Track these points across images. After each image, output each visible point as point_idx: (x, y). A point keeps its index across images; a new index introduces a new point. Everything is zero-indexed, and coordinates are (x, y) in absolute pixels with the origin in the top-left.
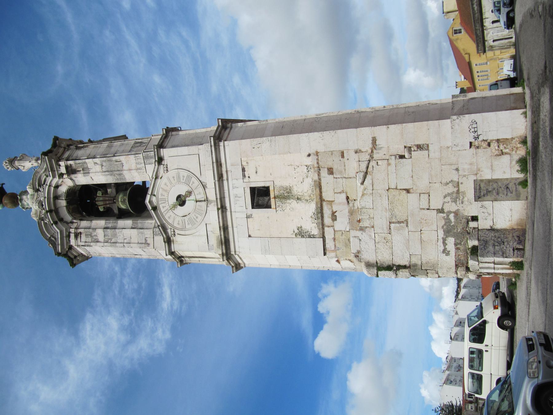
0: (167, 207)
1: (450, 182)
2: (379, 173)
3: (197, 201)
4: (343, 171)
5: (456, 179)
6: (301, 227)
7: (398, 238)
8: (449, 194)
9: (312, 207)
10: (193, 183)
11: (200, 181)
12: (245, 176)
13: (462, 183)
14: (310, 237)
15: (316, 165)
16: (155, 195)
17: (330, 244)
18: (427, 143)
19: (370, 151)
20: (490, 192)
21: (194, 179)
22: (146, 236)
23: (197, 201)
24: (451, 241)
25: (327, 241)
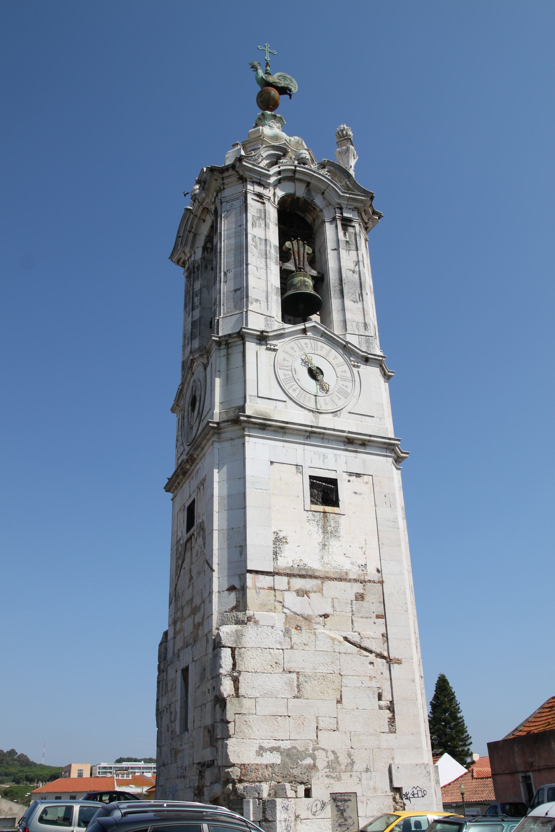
0: (307, 351)
1: (352, 760)
2: (357, 664)
4: (362, 615)
5: (356, 767)
6: (287, 543)
7: (277, 682)
8: (337, 758)
9: (314, 563)
10: (339, 399)
12: (350, 475)
13: (351, 776)
14: (275, 553)
15: (367, 578)
18: (397, 732)
20: (342, 814)
24: (275, 759)
25: (269, 578)
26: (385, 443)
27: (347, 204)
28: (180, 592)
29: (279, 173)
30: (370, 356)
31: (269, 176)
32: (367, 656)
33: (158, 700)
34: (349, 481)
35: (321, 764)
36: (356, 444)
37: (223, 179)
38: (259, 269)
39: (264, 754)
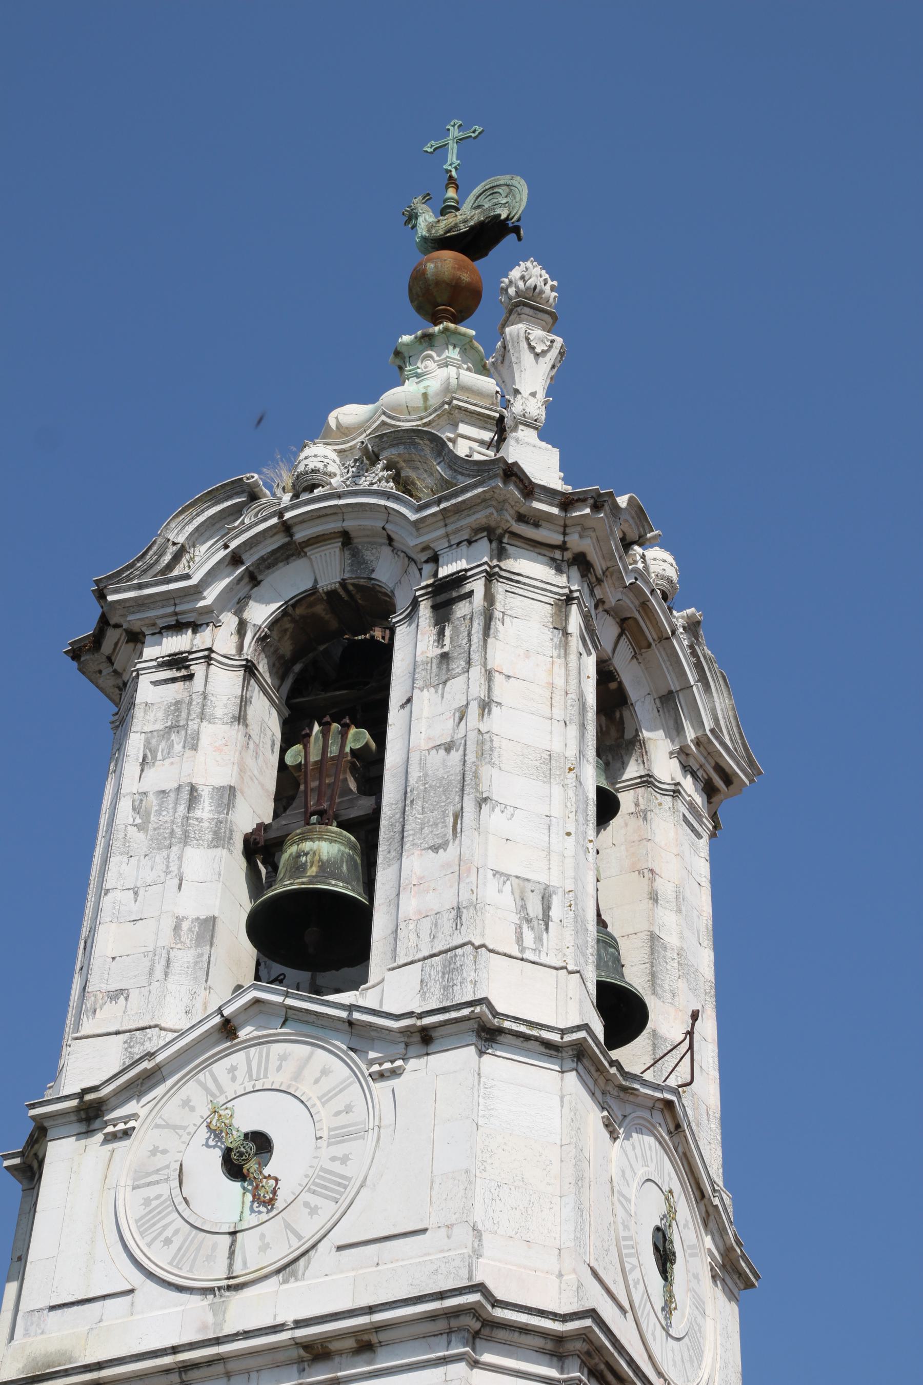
10: (313, 1211)
11: (314, 1246)
21: (328, 1209)
22: (134, 994)
23: (233, 1234)
26: (432, 1317)
27: (447, 535)
29: (235, 559)
30: (427, 1021)
31: (197, 591)
36: (340, 1353)
37: (110, 659)
38: (141, 892)
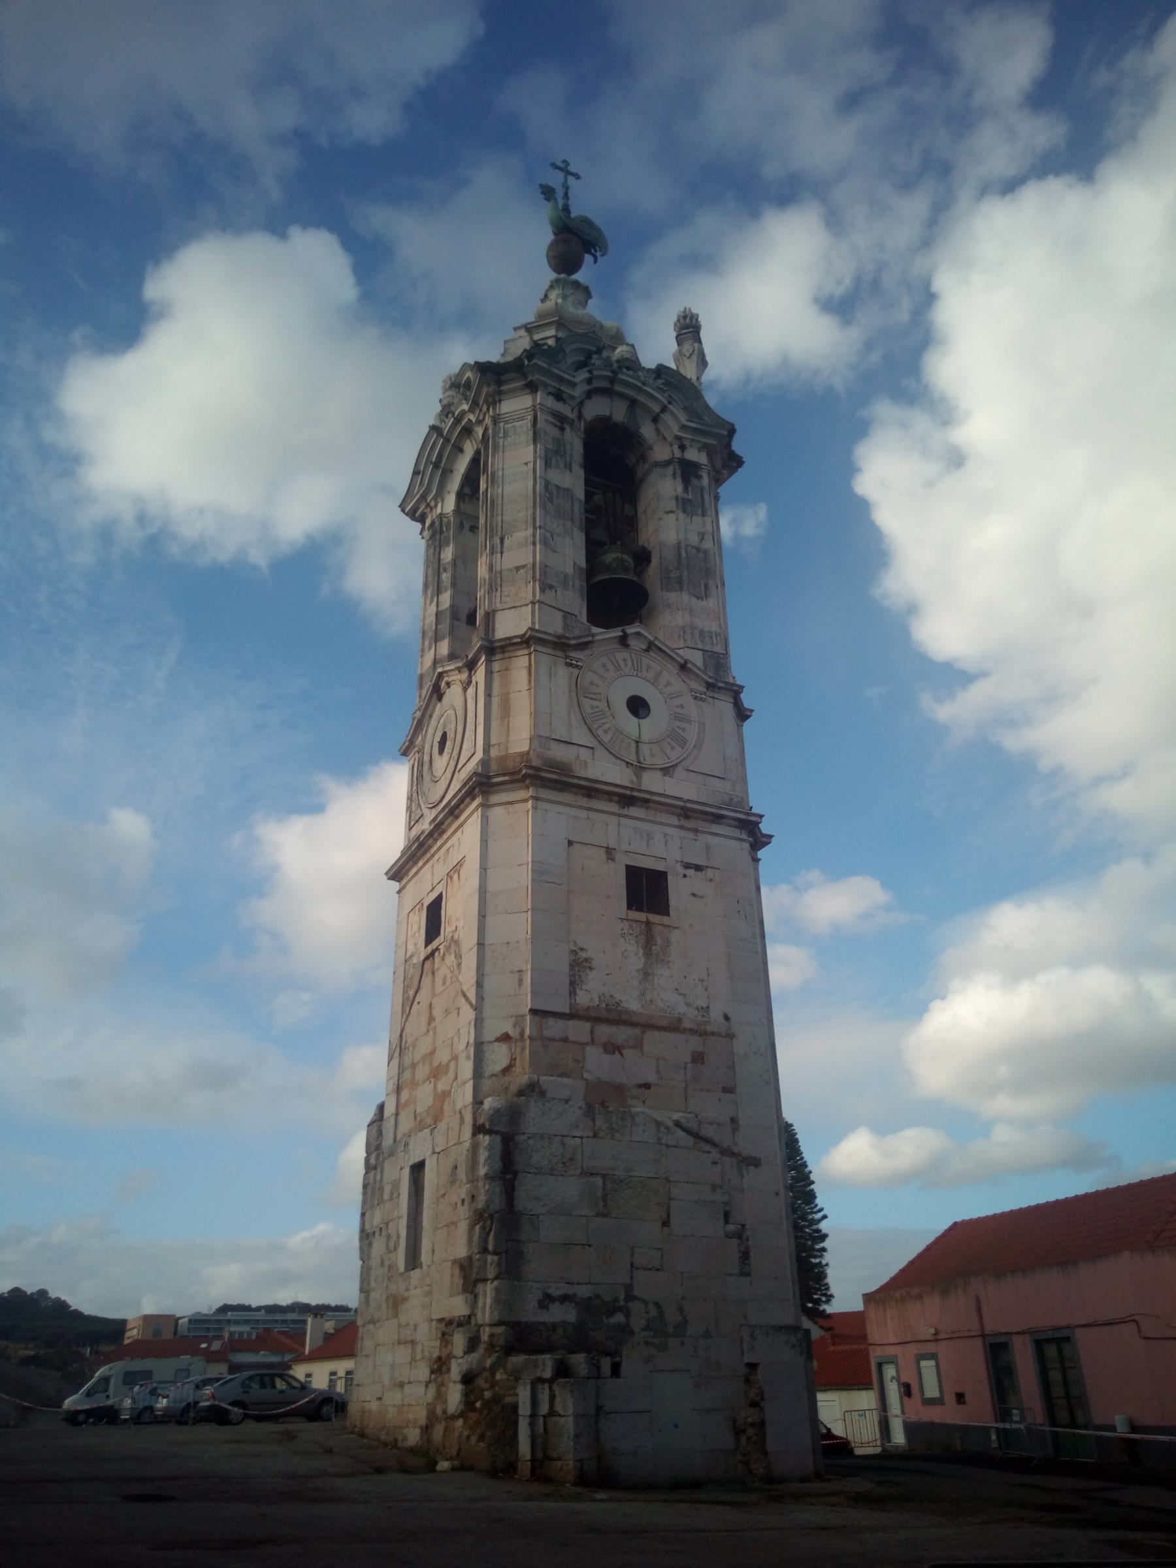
3: (637, 742)
6: (591, 968)
9: (632, 1004)
10: (672, 748)
11: (676, 765)
13: (683, 1344)
14: (573, 984)
15: (709, 1028)
16: (647, 650)
17: (555, 1028)
19: (736, 1150)
28: (409, 1040)
32: (709, 1152)
33: (363, 1214)
34: (685, 876)
35: (637, 1323)
39: (551, 1306)
